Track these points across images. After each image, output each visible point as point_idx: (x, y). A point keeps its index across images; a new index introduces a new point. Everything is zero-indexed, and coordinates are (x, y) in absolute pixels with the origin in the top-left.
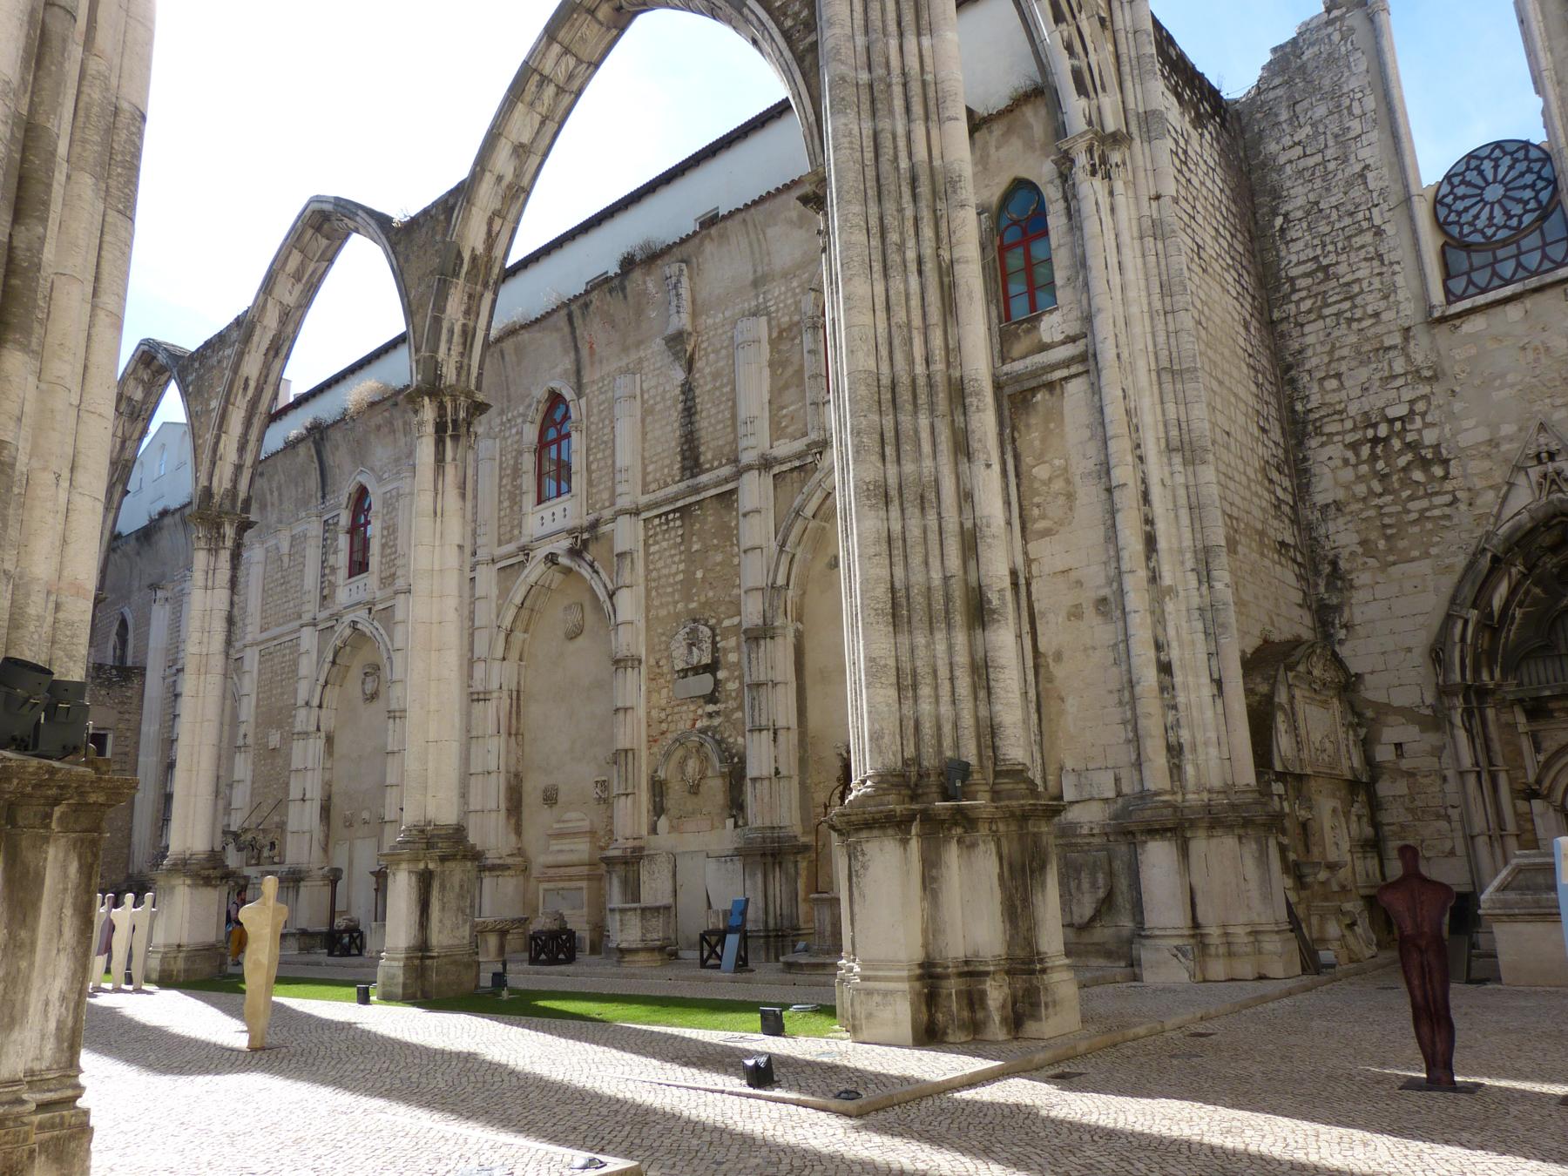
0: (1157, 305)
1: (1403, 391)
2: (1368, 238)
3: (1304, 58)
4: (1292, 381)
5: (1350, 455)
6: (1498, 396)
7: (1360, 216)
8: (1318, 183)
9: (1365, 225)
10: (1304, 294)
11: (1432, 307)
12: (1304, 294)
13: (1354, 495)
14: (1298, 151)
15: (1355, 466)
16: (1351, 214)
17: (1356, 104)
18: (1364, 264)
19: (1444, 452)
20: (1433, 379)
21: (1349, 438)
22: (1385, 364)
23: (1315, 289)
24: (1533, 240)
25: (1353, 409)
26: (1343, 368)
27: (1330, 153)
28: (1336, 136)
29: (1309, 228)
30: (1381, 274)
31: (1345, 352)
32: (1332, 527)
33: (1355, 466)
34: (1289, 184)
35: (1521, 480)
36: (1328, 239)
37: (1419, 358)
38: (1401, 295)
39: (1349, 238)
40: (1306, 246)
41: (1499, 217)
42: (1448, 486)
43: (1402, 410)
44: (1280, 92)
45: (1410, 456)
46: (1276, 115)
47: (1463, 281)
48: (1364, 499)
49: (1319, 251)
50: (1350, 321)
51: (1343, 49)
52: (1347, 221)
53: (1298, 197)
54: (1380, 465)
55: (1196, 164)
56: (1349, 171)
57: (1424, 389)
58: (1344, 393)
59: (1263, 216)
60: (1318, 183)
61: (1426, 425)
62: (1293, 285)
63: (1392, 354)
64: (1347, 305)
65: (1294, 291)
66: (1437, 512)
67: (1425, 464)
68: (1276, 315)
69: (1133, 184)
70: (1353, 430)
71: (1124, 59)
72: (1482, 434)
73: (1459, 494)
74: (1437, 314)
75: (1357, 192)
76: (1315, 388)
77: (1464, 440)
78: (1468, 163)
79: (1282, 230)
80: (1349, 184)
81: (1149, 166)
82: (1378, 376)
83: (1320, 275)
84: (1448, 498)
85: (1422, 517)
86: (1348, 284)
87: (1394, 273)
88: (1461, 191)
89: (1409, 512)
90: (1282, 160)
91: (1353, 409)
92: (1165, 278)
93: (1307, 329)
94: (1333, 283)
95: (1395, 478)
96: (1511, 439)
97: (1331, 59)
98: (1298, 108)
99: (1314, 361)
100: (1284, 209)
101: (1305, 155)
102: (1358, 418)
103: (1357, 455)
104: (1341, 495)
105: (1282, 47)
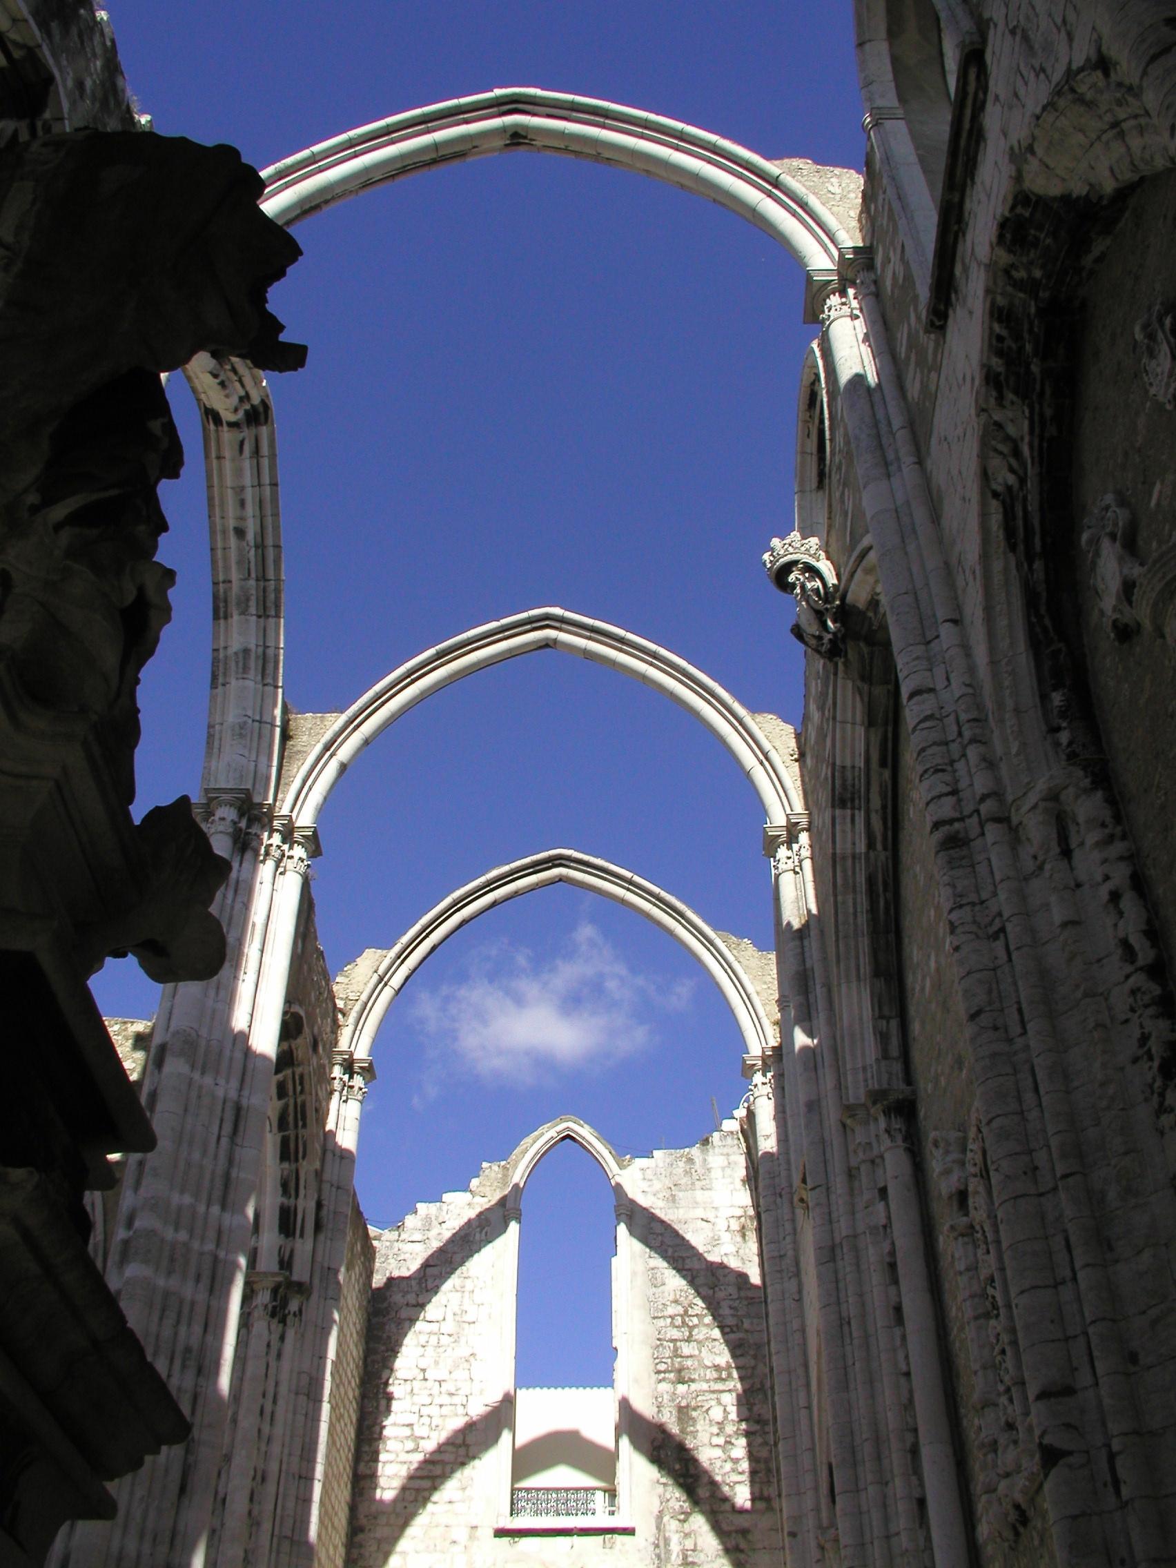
36: (425, 1411)
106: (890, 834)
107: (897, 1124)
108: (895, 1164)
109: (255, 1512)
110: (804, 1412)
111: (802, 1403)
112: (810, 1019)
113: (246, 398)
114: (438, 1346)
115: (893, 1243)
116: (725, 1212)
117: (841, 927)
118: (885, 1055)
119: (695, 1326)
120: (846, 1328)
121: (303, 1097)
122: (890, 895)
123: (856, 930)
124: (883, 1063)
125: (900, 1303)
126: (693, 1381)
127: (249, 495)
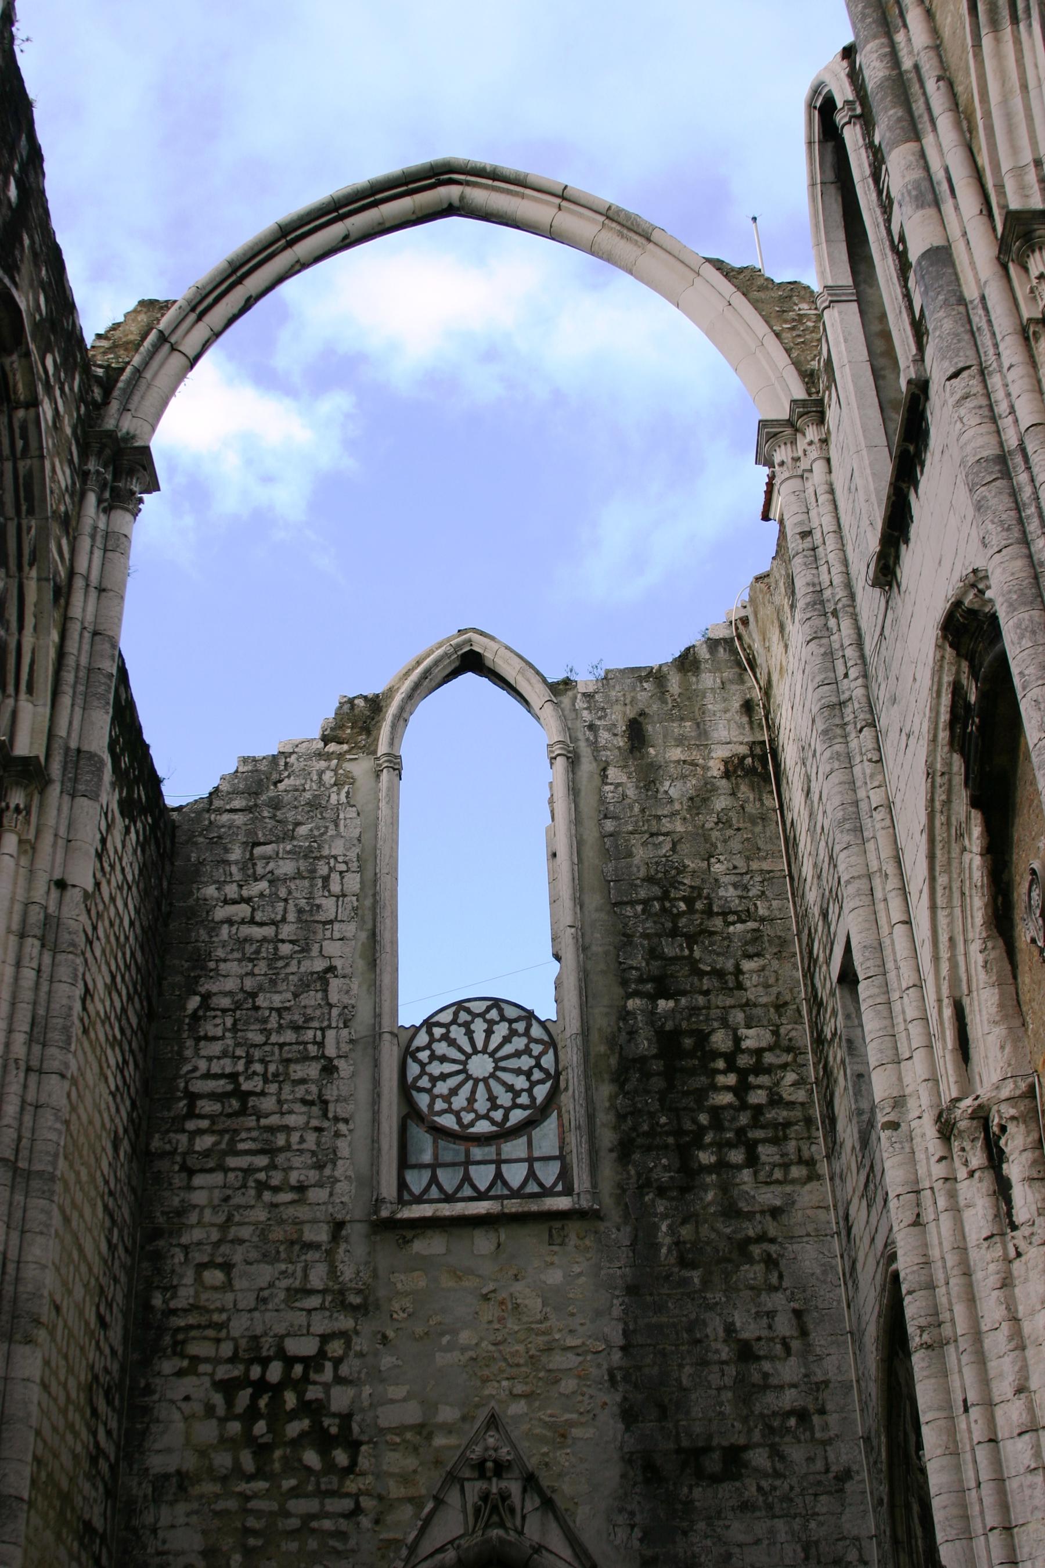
1: (316, 1317)
3: (281, 786)
4: (157, 1257)
5: (218, 1399)
6: (442, 1359)
7: (310, 1034)
8: (262, 967)
9: (313, 1050)
10: (204, 1124)
11: (379, 1202)
12: (204, 1124)
13: (211, 1469)
15: (223, 1421)
16: (297, 1028)
17: (335, 877)
18: (298, 1107)
19: (355, 1428)
20: (360, 1310)
21: (223, 1372)
22: (300, 1267)
24: (515, 1148)
25: (239, 1326)
26: (237, 1258)
27: (287, 931)
28: (300, 911)
29: (234, 1029)
30: (318, 1130)
31: (245, 1232)
32: (165, 1516)
33: (223, 1421)
34: (220, 953)
35: (453, 1498)
36: (257, 1054)
37: (348, 1273)
38: (342, 1169)
39: (288, 1061)
40: (225, 1054)
41: (482, 1105)
42: (351, 1486)
43: (306, 1347)
44: (239, 819)
45: (305, 1424)
46: (227, 850)
47: (426, 1175)
48: (224, 1479)
49: (240, 1067)
50: (263, 1186)
51: (334, 798)
52: (289, 1036)
53: (229, 978)
54: (260, 1427)
55: (112, 866)
56: (306, 966)
57: (345, 1322)
58: (229, 1297)
60: (262, 967)
61: (339, 1380)
62: (191, 1106)
63: (311, 1255)
64: (262, 1161)
65: (191, 1114)
66: (327, 1524)
67: (324, 1442)
68: (156, 1144)
70: (233, 1360)
71: (71, 661)
72: (412, 1414)
73: (366, 1502)
74: (385, 1213)
75: (312, 998)
76: (189, 1278)
77: (388, 1417)
78: (456, 1014)
79: (195, 1017)
80: (304, 986)
81: (62, 832)
82: (284, 1283)
83: (235, 1104)
84: (348, 1504)
85: (306, 1526)
86: (272, 1130)
87: (337, 1135)
88: (441, 1048)
89: (287, 1515)
90: (221, 913)
91: (239, 1326)
92: (41, 1012)
93: (198, 1180)
95: (278, 1454)
96: (448, 1429)
97: (315, 805)
98: (258, 851)
99: (197, 1234)
100: (206, 986)
101: (252, 922)
102: (243, 1343)
103: (230, 1403)
104: (190, 1462)
105: (254, 760)
110: (900, 930)
111: (897, 915)
114: (277, 957)
119: (681, 914)
126: (684, 993)
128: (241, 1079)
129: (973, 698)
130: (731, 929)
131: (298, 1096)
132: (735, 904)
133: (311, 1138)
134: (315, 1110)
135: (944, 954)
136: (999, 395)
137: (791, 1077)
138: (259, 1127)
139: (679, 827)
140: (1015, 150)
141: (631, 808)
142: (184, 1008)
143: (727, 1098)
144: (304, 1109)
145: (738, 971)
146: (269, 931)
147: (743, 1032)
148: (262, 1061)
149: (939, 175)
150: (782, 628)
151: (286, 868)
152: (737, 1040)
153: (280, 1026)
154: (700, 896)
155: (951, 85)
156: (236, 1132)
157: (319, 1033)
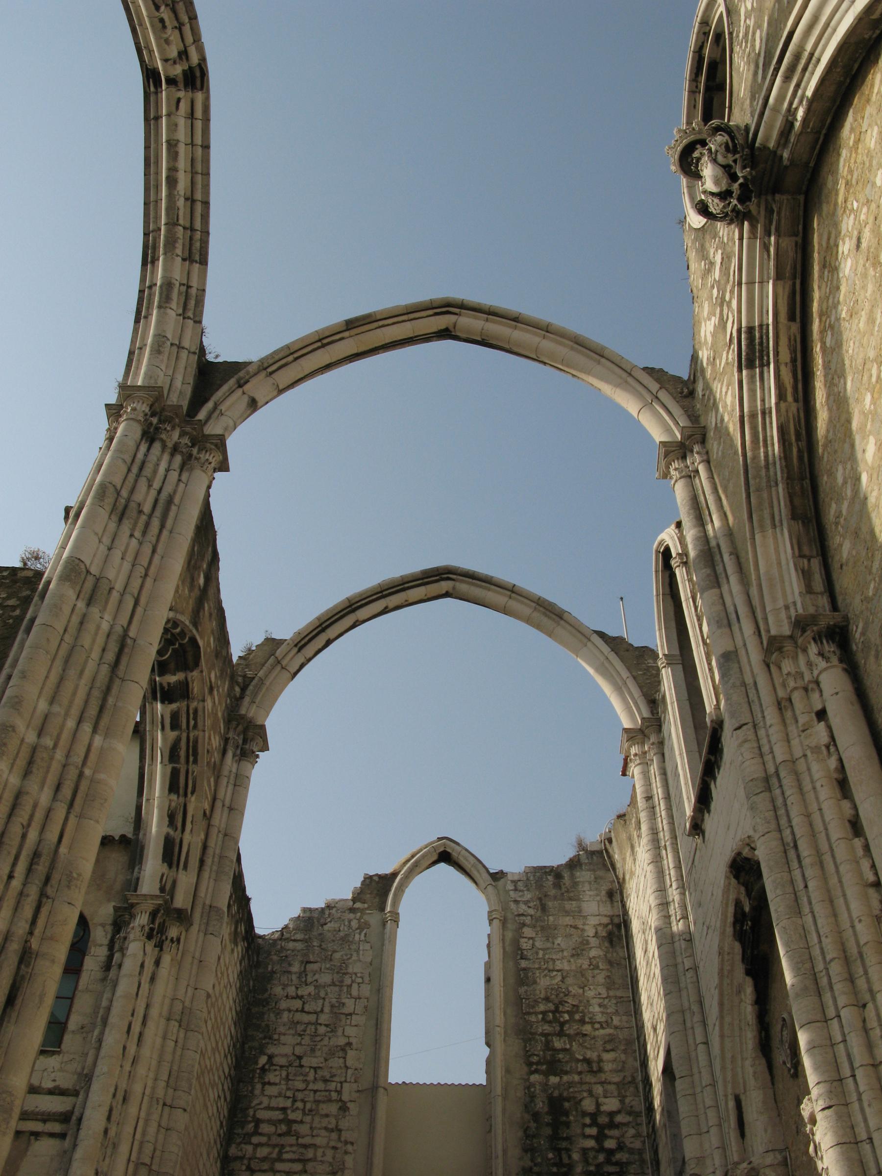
0: (160, 1093)
2: (333, 1109)
3: (326, 927)
7: (332, 1086)
8: (307, 1040)
9: (334, 1095)
10: (264, 1139)
12: (264, 1139)
14: (298, 1004)
16: (326, 1081)
17: (355, 986)
18: (323, 1133)
23: (275, 1140)
27: (324, 1018)
28: (332, 1006)
29: (287, 1079)
34: (282, 1029)
36: (300, 1095)
39: (318, 1102)
40: (280, 1095)
44: (299, 946)
46: (290, 965)
49: (288, 1103)
51: (357, 936)
52: (320, 1086)
53: (285, 1047)
55: (222, 974)
59: (251, 1048)
60: (307, 1040)
62: (257, 1126)
65: (256, 1133)
68: (233, 1151)
69: (179, 964)
71: (210, 851)
75: (336, 1062)
79: (263, 1069)
80: (331, 1053)
81: (197, 955)
83: (284, 1128)
86: (305, 1146)
87: (346, 1153)
92: (175, 1068)
94: (292, 1140)
97: (345, 940)
98: (310, 967)
100: (271, 1050)
101: (303, 1011)
105: (310, 910)
106: (800, 386)
107: (829, 648)
108: (833, 681)
109: (112, 1133)
110: (701, 1048)
111: (699, 1039)
112: (719, 585)
113: (184, 54)
114: (316, 1034)
115: (840, 760)
116: (593, 921)
117: (751, 482)
118: (809, 589)
119: (566, 1022)
120: (792, 854)
121: (196, 733)
122: (803, 444)
123: (768, 481)
124: (808, 596)
125: (857, 815)
126: (566, 1073)
127: (182, 149)
128: (289, 1112)
129: (747, 909)
130: (597, 1033)
131: (324, 1125)
132: (599, 1018)
133: (330, 1153)
134: (334, 1135)
135: (729, 1066)
136: (764, 741)
137: (632, 1132)
138: (298, 1145)
139: (566, 966)
140: (774, 600)
141: (537, 953)
142: (256, 1063)
143: (591, 1143)
144: (327, 1134)
145: (600, 1060)
146: (312, 1018)
147: (601, 1100)
148: (303, 1101)
149: (731, 609)
150: (632, 847)
151: (325, 978)
152: (598, 1105)
153: (315, 1079)
154: (577, 1012)
155: (738, 558)
156: (283, 1146)
157: (339, 1085)
